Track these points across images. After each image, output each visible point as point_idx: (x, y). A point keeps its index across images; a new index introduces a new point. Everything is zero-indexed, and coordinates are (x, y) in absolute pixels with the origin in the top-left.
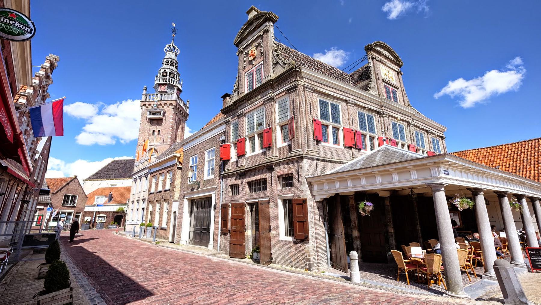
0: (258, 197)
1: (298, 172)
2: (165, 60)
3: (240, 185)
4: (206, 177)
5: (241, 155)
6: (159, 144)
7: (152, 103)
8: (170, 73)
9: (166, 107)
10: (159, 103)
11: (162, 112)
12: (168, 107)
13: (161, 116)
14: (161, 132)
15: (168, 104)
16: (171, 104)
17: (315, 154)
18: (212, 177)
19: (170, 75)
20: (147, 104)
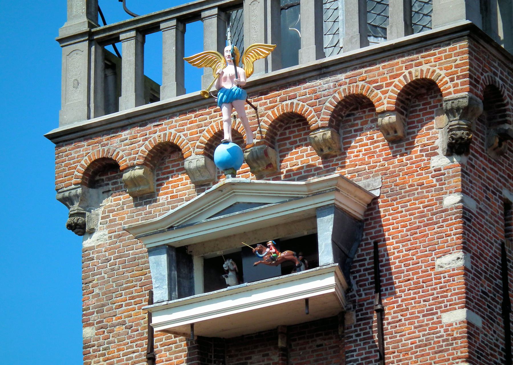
7: (186, 132)
9: (367, 148)
10: (270, 108)
12: (400, 140)
13: (319, 284)
16: (419, 97)
20: (129, 148)
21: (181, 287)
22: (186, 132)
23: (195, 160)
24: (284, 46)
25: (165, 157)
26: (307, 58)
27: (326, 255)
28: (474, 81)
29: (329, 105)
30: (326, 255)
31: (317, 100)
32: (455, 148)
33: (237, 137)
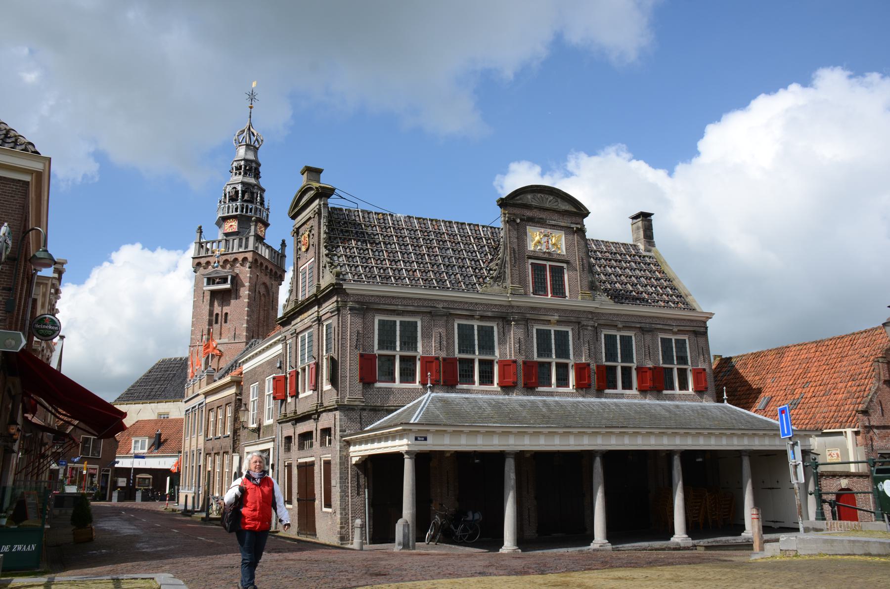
2: (235, 164)
4: (268, 422)
5: (296, 395)
6: (226, 340)
7: (211, 260)
8: (243, 193)
10: (224, 258)
11: (229, 278)
13: (227, 286)
14: (229, 317)
15: (240, 259)
16: (245, 259)
18: (271, 421)
21: (208, 284)
22: (211, 260)
24: (227, 247)
25: (208, 263)
26: (230, 251)
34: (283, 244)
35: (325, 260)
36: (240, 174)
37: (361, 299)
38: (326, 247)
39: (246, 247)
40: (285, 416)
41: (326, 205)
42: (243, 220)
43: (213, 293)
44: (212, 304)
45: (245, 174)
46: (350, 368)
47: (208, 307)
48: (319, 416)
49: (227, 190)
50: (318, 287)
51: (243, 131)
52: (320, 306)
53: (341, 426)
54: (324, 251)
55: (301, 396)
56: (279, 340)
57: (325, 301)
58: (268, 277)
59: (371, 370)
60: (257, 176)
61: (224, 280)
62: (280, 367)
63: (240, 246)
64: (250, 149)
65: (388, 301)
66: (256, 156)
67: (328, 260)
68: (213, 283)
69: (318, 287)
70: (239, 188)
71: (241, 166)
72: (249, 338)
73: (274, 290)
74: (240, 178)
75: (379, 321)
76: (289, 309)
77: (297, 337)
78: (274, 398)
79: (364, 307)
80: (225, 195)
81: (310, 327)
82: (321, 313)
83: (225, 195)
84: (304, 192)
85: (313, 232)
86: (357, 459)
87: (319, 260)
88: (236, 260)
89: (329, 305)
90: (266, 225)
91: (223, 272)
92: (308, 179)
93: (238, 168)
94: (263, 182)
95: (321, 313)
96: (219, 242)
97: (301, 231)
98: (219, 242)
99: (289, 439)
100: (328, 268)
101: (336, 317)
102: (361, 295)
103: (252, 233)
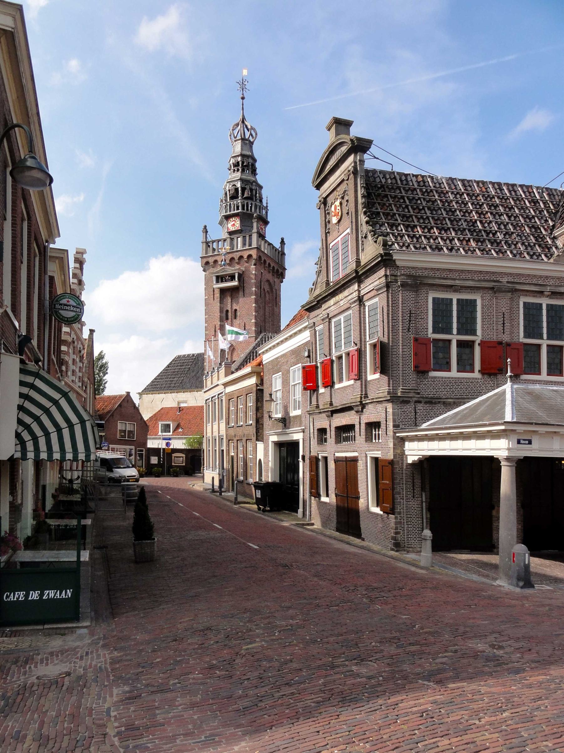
0: (345, 452)
1: (386, 421)
2: (232, 161)
3: (328, 430)
5: (329, 384)
8: (243, 189)
10: (230, 256)
13: (235, 283)
14: (238, 314)
15: (245, 257)
16: (250, 256)
17: (411, 395)
18: (298, 412)
19: (243, 194)
20: (211, 260)
21: (217, 282)
23: (220, 263)
26: (235, 250)
27: (236, 279)
28: (257, 255)
29: (238, 256)
30: (236, 279)
31: (236, 256)
32: (255, 265)
33: (225, 260)
34: (282, 242)
35: (365, 228)
36: (238, 170)
37: (413, 272)
38: (365, 213)
39: (250, 245)
40: (318, 407)
41: (362, 162)
42: (246, 217)
43: (223, 291)
44: (222, 301)
45: (243, 171)
46: (403, 353)
47: (219, 304)
48: (362, 409)
49: (227, 189)
50: (358, 262)
51: (237, 125)
52: (360, 282)
53: (394, 421)
54: (363, 219)
55: (337, 386)
56: (305, 328)
57: (367, 277)
58: (271, 274)
59: (427, 357)
60: (254, 172)
61: (232, 278)
62: (309, 356)
63: (244, 244)
64: (246, 144)
65: (444, 275)
66: (251, 151)
67: (371, 228)
68: (222, 281)
69: (358, 262)
70: (239, 185)
71: (238, 163)
72: (258, 333)
73: (276, 287)
74: (238, 175)
75: (434, 299)
76: (317, 292)
77: (330, 322)
78: (305, 389)
79: (416, 282)
80: (226, 194)
81: (348, 308)
82: (362, 293)
83: (226, 194)
84: (332, 152)
85: (346, 198)
86: (416, 458)
87: (357, 230)
88: (241, 257)
89: (376, 280)
90: (266, 223)
91: (230, 270)
92: (337, 134)
93: (236, 165)
94: (260, 179)
95: (362, 293)
96: (225, 240)
97: (329, 200)
98: (225, 240)
99: (322, 431)
100: (370, 237)
101: (385, 295)
102: (413, 268)
103: (255, 230)
